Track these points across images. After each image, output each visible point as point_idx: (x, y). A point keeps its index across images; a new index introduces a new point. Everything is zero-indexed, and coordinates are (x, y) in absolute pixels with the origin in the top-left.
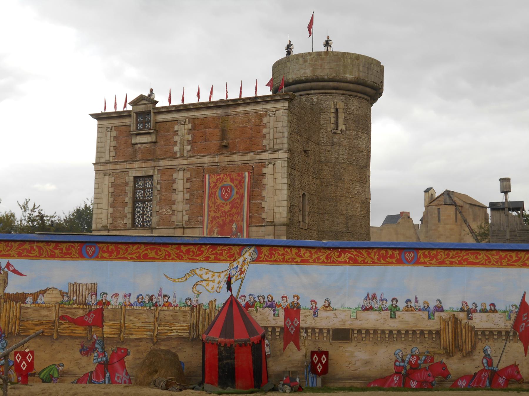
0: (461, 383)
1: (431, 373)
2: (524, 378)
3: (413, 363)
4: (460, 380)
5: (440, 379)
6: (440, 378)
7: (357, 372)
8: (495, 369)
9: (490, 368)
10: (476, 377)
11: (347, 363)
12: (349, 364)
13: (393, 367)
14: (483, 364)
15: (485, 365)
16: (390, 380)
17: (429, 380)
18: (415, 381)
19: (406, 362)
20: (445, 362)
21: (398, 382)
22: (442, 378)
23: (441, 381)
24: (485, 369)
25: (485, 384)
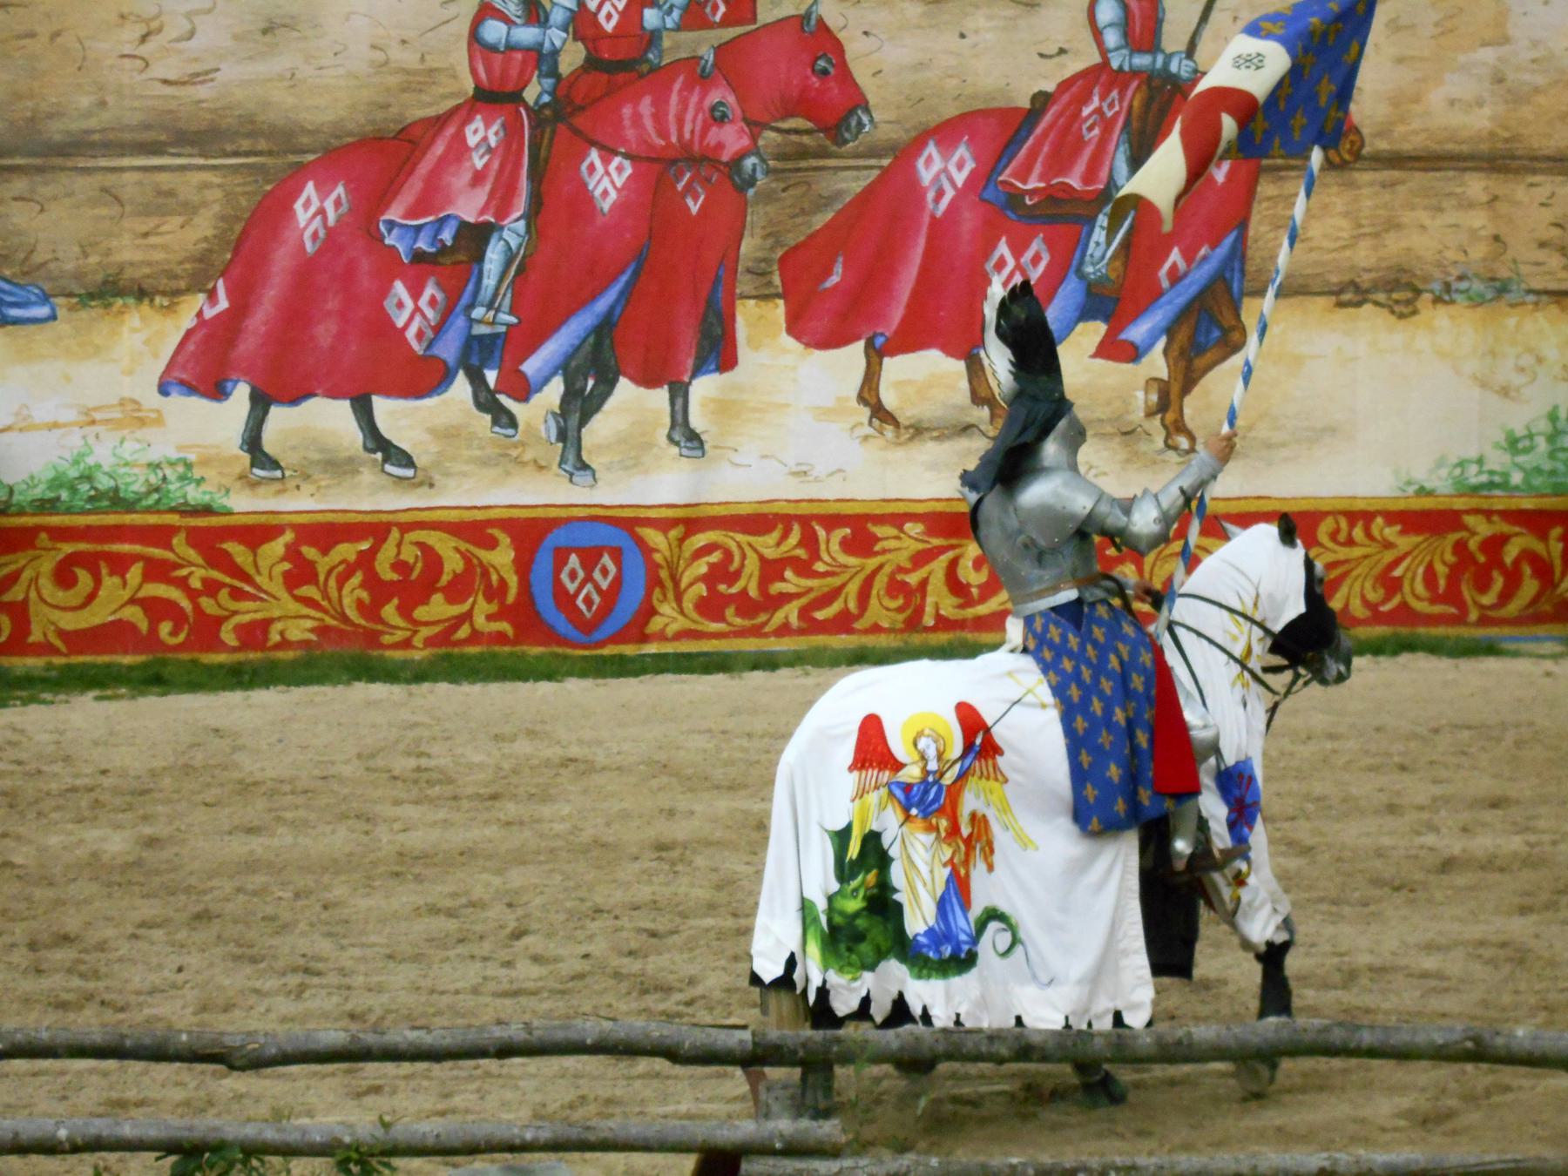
0: (938, 164)
1: (731, 99)
2: (1365, 131)
3: (609, 27)
4: (931, 149)
5: (794, 138)
6: (797, 132)
7: (202, 92)
8: (1174, 68)
9: (1142, 61)
10: (1048, 118)
11: (133, 32)
12: (144, 39)
13: (460, 57)
14: (1097, 34)
15: (1112, 38)
16: (439, 148)
17: (720, 146)
18: (617, 153)
19: (558, 16)
20: (832, 21)
21: (496, 165)
22: (808, 132)
23: (803, 153)
24: (1106, 63)
25: (1104, 174)
